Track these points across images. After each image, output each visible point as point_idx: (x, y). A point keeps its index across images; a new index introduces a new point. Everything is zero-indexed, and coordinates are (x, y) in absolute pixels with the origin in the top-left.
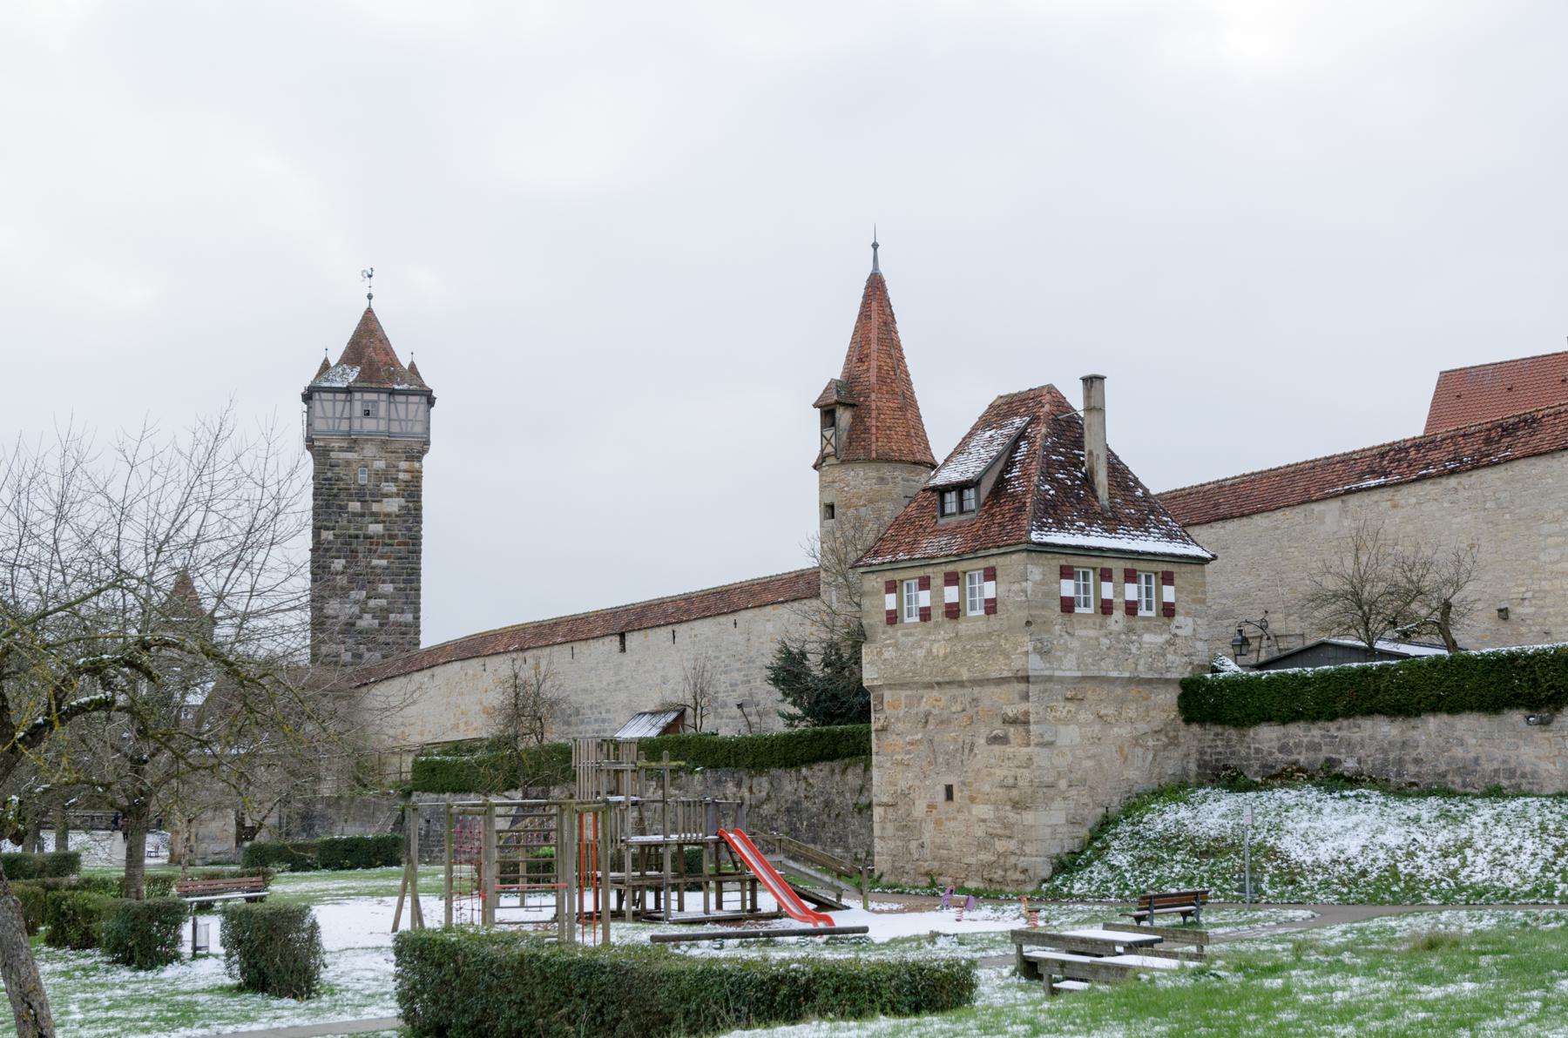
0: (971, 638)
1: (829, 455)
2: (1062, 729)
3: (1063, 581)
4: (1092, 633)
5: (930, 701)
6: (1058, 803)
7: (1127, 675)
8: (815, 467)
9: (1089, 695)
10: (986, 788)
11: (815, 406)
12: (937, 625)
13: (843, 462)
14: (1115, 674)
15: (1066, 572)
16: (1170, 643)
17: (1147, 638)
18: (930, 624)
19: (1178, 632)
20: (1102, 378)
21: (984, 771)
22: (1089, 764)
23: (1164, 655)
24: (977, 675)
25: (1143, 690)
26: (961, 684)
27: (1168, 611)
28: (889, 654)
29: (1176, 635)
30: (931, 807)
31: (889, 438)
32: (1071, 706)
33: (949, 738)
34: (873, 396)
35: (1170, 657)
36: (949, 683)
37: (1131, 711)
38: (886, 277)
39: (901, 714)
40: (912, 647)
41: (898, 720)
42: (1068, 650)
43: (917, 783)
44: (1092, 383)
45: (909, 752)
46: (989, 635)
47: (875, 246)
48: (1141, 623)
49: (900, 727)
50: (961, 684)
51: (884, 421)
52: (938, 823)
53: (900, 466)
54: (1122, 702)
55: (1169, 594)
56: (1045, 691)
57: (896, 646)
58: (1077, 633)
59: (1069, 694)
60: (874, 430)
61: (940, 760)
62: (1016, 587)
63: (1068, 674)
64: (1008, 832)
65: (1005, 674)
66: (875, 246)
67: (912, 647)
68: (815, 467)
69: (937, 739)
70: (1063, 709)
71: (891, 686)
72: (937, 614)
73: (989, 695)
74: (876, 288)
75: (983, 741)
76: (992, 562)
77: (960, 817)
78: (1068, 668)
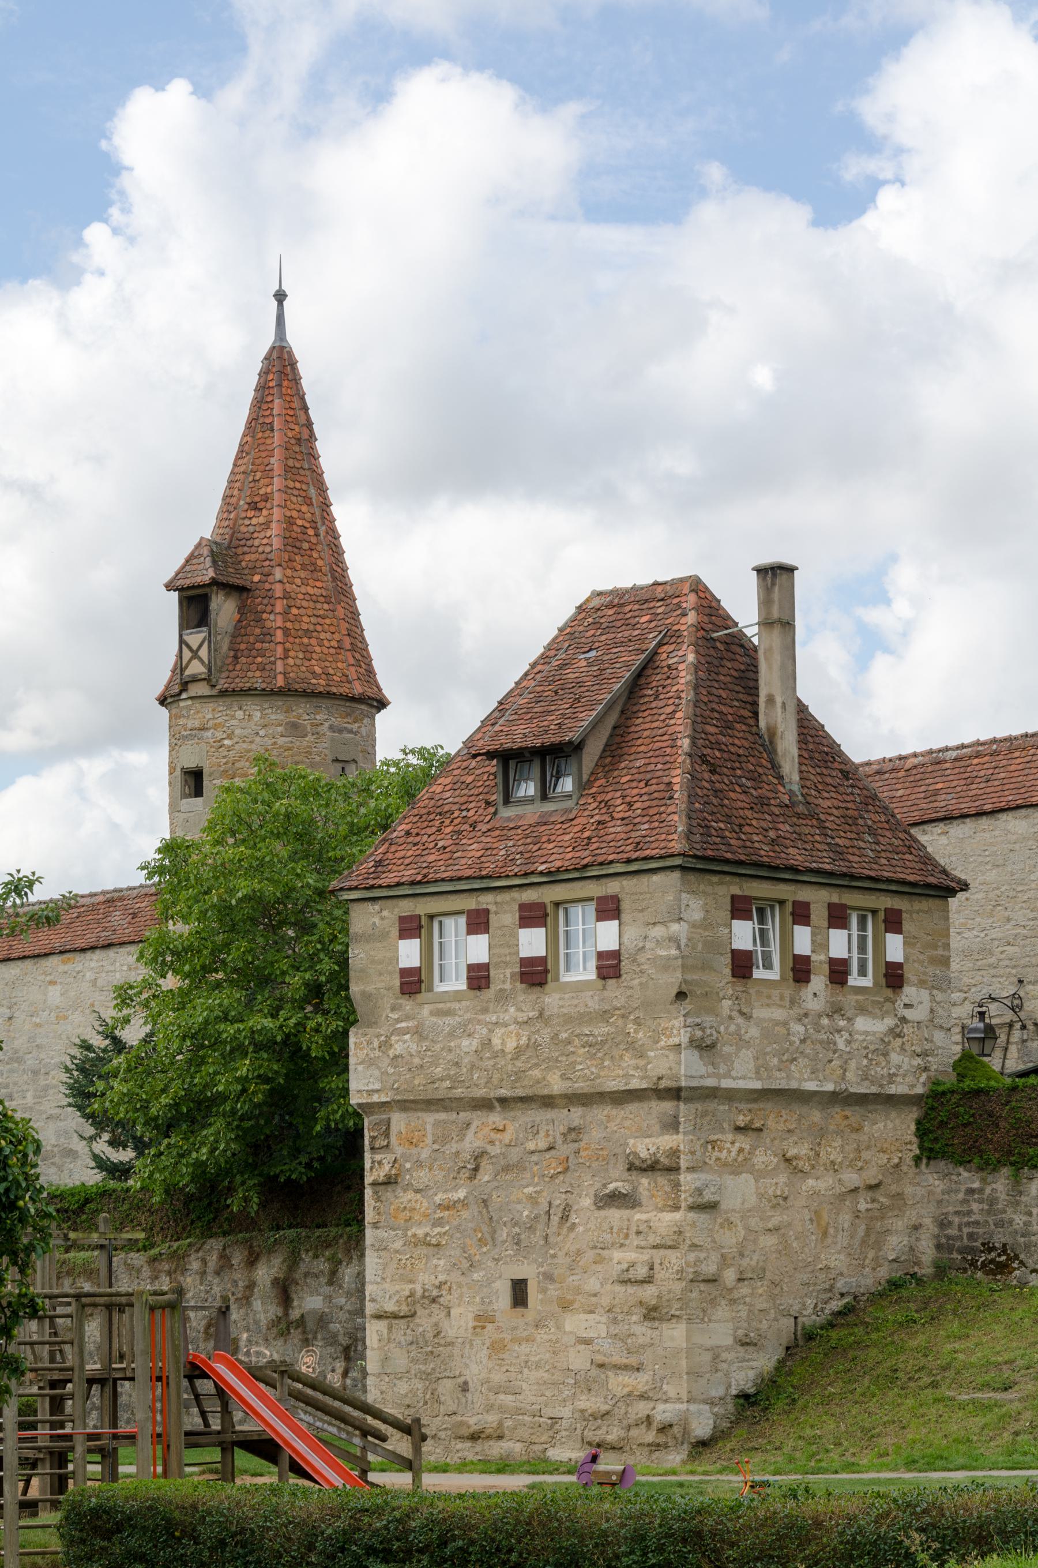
0: (568, 1019)
1: (195, 679)
2: (729, 1180)
3: (736, 924)
4: (779, 1014)
5: (480, 1132)
6: (722, 1311)
7: (829, 1087)
8: (163, 701)
9: (771, 1123)
10: (593, 1284)
11: (169, 587)
12: (503, 997)
13: (223, 694)
14: (811, 1086)
15: (740, 909)
16: (895, 1033)
17: (862, 1023)
18: (490, 993)
19: (908, 1014)
20: (790, 570)
21: (590, 1255)
22: (769, 1241)
23: (886, 1055)
24: (581, 1086)
25: (854, 1114)
26: (548, 1102)
27: (894, 977)
29: (904, 1020)
30: (483, 1319)
31: (308, 651)
32: (744, 1142)
33: (521, 1198)
34: (278, 573)
35: (895, 1058)
37: (833, 1151)
38: (298, 354)
39: (425, 1154)
40: (451, 1035)
41: (419, 1164)
42: (742, 1042)
43: (455, 1277)
44: (775, 577)
45: (439, 1222)
46: (605, 1015)
47: (280, 297)
48: (852, 999)
49: (422, 1177)
50: (548, 1102)
51: (298, 618)
52: (497, 1348)
53: (325, 703)
54: (821, 1134)
55: (895, 948)
56: (705, 1113)
57: (418, 1032)
58: (756, 1013)
59: (741, 1120)
60: (279, 636)
61: (503, 1234)
62: (658, 932)
63: (741, 1084)
64: (633, 1361)
65: (636, 1084)
67: (451, 1035)
68: (163, 701)
69: (496, 1200)
70: (733, 1145)
71: (405, 1105)
72: (503, 978)
73: (604, 1125)
74: (280, 371)
75: (587, 1202)
76: (613, 887)
77: (541, 1336)
78: (742, 1074)
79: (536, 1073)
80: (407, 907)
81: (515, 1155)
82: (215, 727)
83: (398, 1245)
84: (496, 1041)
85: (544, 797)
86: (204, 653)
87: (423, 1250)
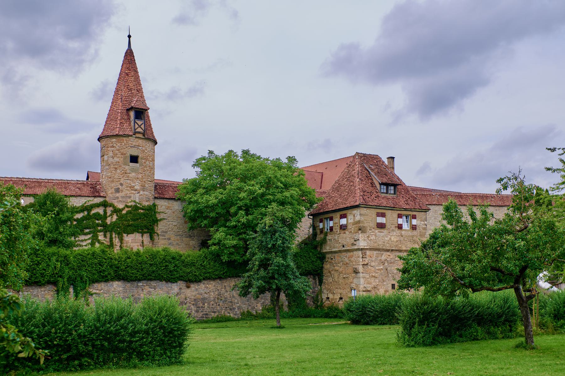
1: (139, 133)
5: (385, 256)
13: (146, 139)
28: (373, 237)
36: (396, 250)
39: (373, 259)
43: (380, 283)
45: (377, 273)
47: (129, 37)
49: (373, 264)
61: (390, 275)
62: (423, 222)
66: (129, 37)
67: (383, 237)
69: (389, 269)
71: (370, 249)
74: (129, 55)
79: (400, 246)
80: (399, 212)
81: (392, 261)
82: (142, 146)
83: (368, 277)
84: (392, 238)
85: (387, 193)
86: (143, 126)
87: (373, 278)
